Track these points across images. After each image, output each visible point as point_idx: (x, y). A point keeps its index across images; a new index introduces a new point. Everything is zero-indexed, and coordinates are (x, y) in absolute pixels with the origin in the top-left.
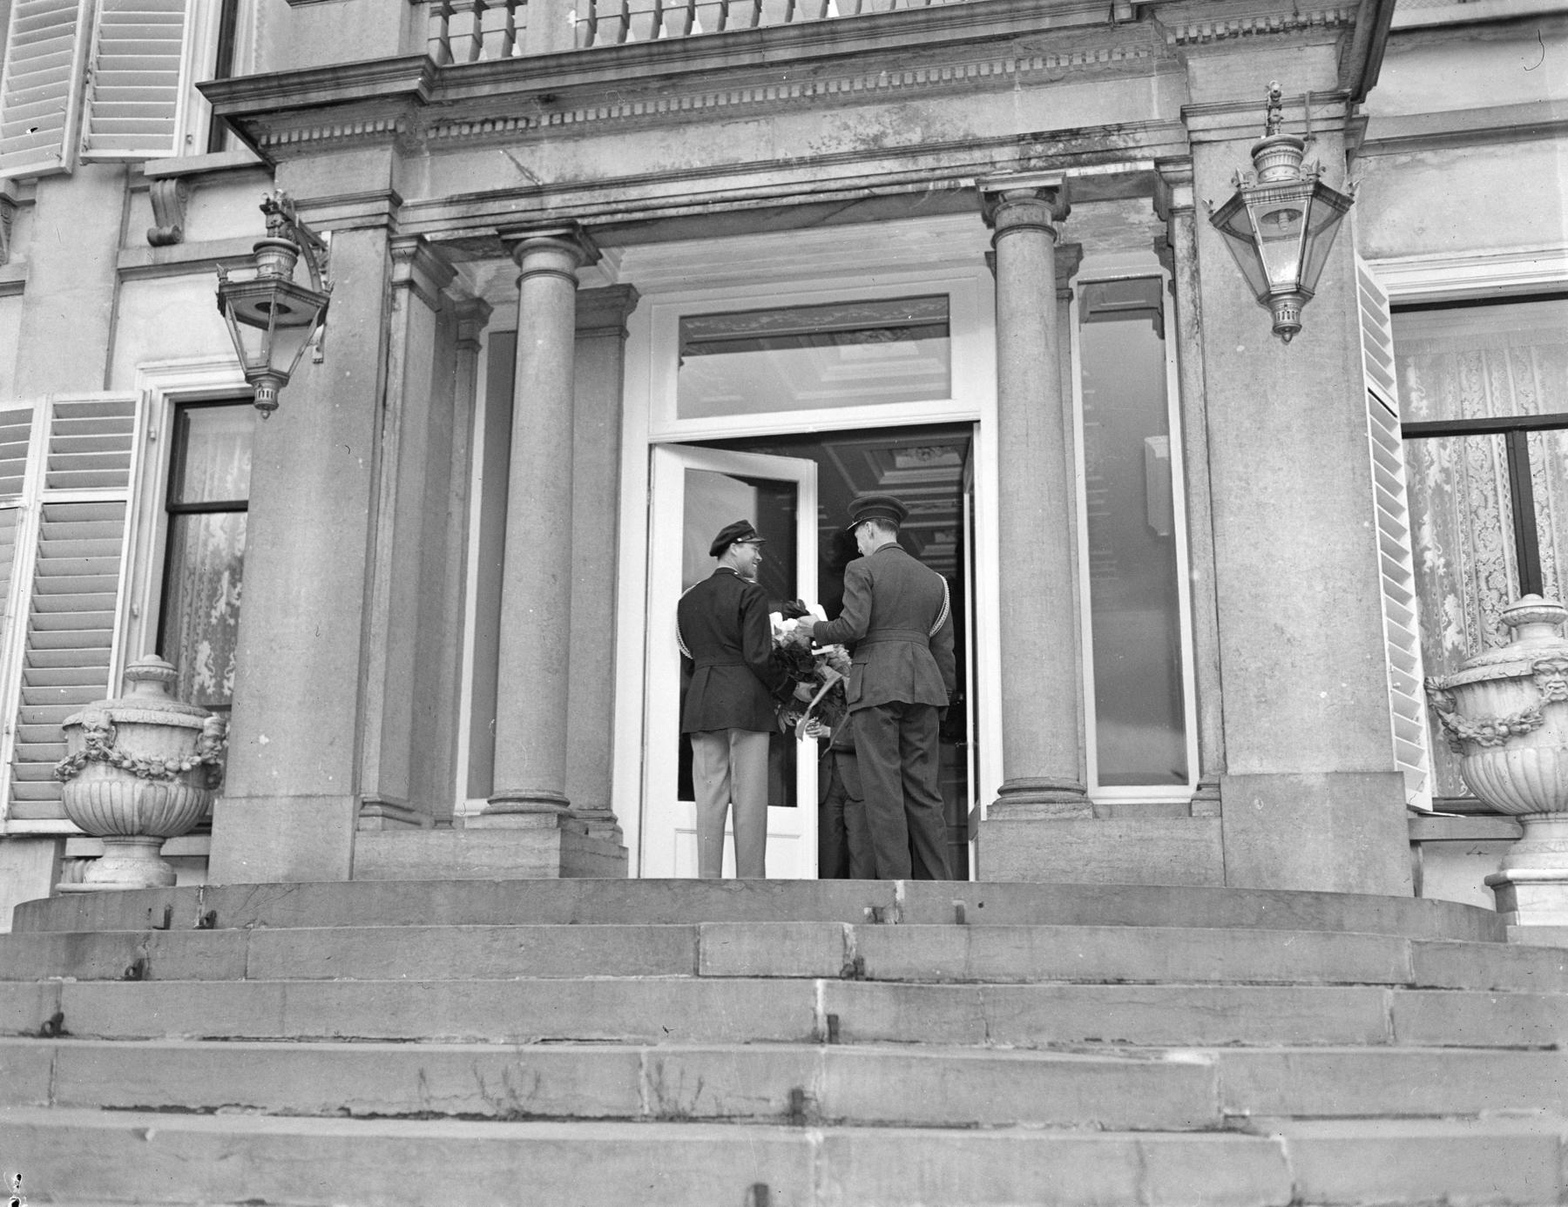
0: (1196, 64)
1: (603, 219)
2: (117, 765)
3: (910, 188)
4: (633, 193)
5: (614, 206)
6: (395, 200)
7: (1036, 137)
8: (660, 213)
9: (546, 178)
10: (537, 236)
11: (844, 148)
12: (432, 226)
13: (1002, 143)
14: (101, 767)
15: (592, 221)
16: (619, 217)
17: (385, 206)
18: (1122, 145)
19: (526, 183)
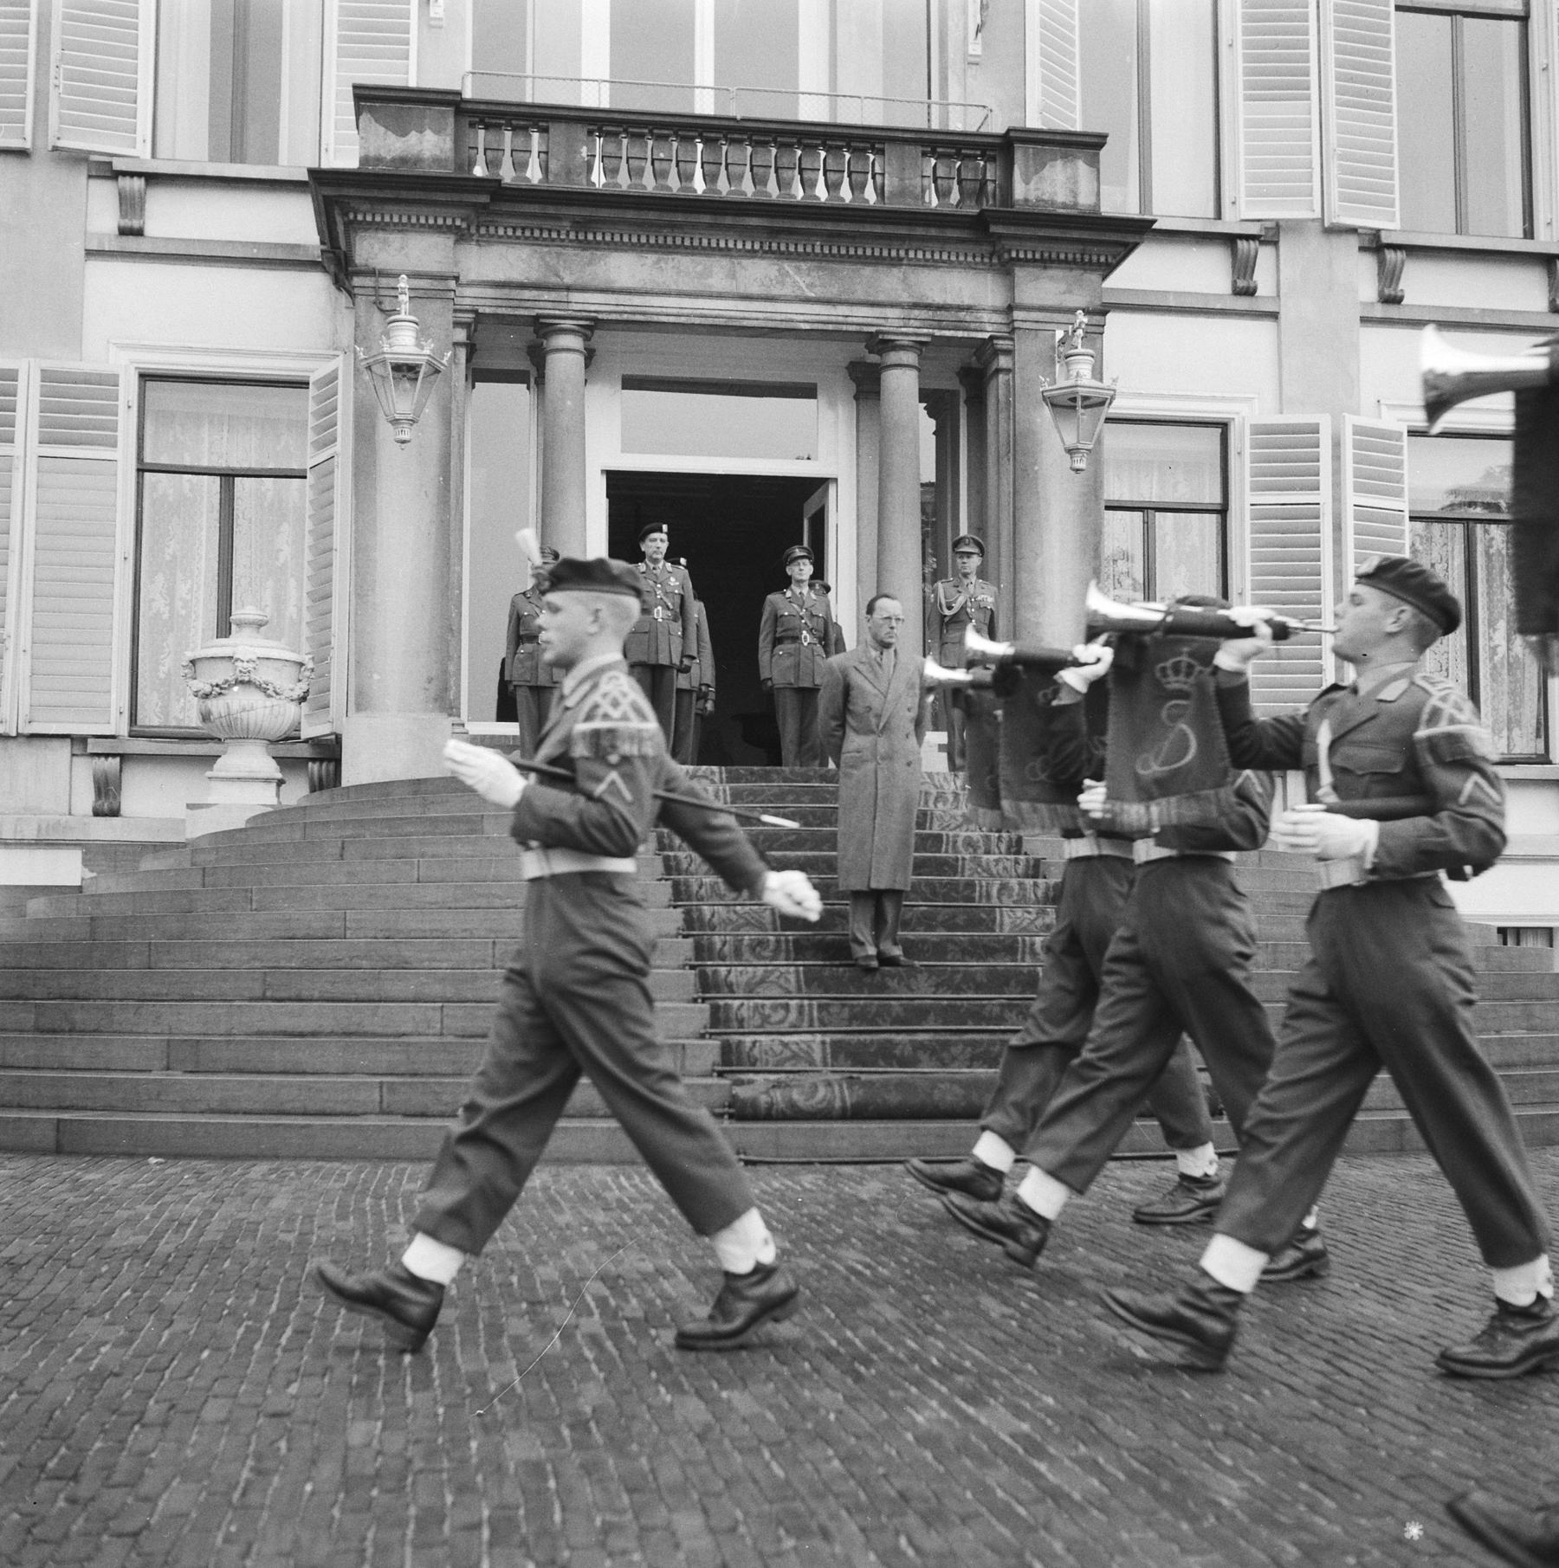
0: (1020, 273)
1: (614, 317)
3: (830, 327)
4: (637, 300)
5: (621, 308)
6: (457, 278)
7: (915, 306)
8: (655, 318)
9: (568, 279)
10: (568, 324)
11: (787, 291)
12: (483, 302)
13: (892, 305)
15: (605, 316)
16: (625, 317)
17: (452, 284)
18: (968, 318)
19: (553, 280)
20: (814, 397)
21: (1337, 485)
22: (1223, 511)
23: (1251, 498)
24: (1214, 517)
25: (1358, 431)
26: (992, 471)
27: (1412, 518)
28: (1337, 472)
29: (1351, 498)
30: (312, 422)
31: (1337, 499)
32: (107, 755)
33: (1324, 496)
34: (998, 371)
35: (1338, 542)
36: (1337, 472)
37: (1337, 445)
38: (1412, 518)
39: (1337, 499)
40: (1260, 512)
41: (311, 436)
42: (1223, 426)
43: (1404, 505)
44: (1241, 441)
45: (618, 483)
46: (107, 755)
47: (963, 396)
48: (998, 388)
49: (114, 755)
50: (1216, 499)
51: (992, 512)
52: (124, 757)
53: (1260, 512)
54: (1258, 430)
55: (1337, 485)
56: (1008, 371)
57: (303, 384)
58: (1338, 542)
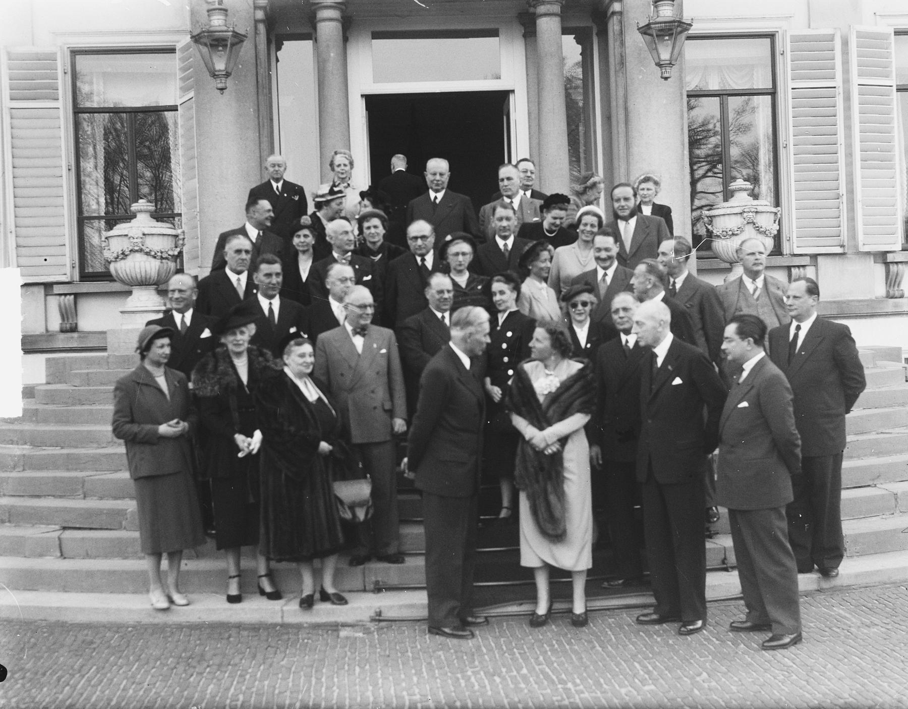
2: (148, 254)
20: (497, 35)
21: (846, 71)
22: (773, 93)
24: (770, 97)
25: (860, 35)
26: (612, 79)
27: (898, 90)
28: (846, 63)
29: (856, 80)
30: (179, 75)
31: (846, 81)
32: (65, 295)
33: (838, 82)
34: (614, 13)
35: (848, 109)
36: (846, 63)
37: (845, 43)
38: (898, 90)
39: (846, 81)
41: (179, 84)
42: (771, 36)
43: (894, 82)
44: (784, 44)
45: (373, 102)
46: (65, 295)
47: (595, 32)
48: (613, 26)
49: (70, 294)
51: (613, 104)
52: (76, 295)
54: (796, 39)
55: (846, 71)
56: (621, 13)
57: (172, 50)
58: (848, 109)
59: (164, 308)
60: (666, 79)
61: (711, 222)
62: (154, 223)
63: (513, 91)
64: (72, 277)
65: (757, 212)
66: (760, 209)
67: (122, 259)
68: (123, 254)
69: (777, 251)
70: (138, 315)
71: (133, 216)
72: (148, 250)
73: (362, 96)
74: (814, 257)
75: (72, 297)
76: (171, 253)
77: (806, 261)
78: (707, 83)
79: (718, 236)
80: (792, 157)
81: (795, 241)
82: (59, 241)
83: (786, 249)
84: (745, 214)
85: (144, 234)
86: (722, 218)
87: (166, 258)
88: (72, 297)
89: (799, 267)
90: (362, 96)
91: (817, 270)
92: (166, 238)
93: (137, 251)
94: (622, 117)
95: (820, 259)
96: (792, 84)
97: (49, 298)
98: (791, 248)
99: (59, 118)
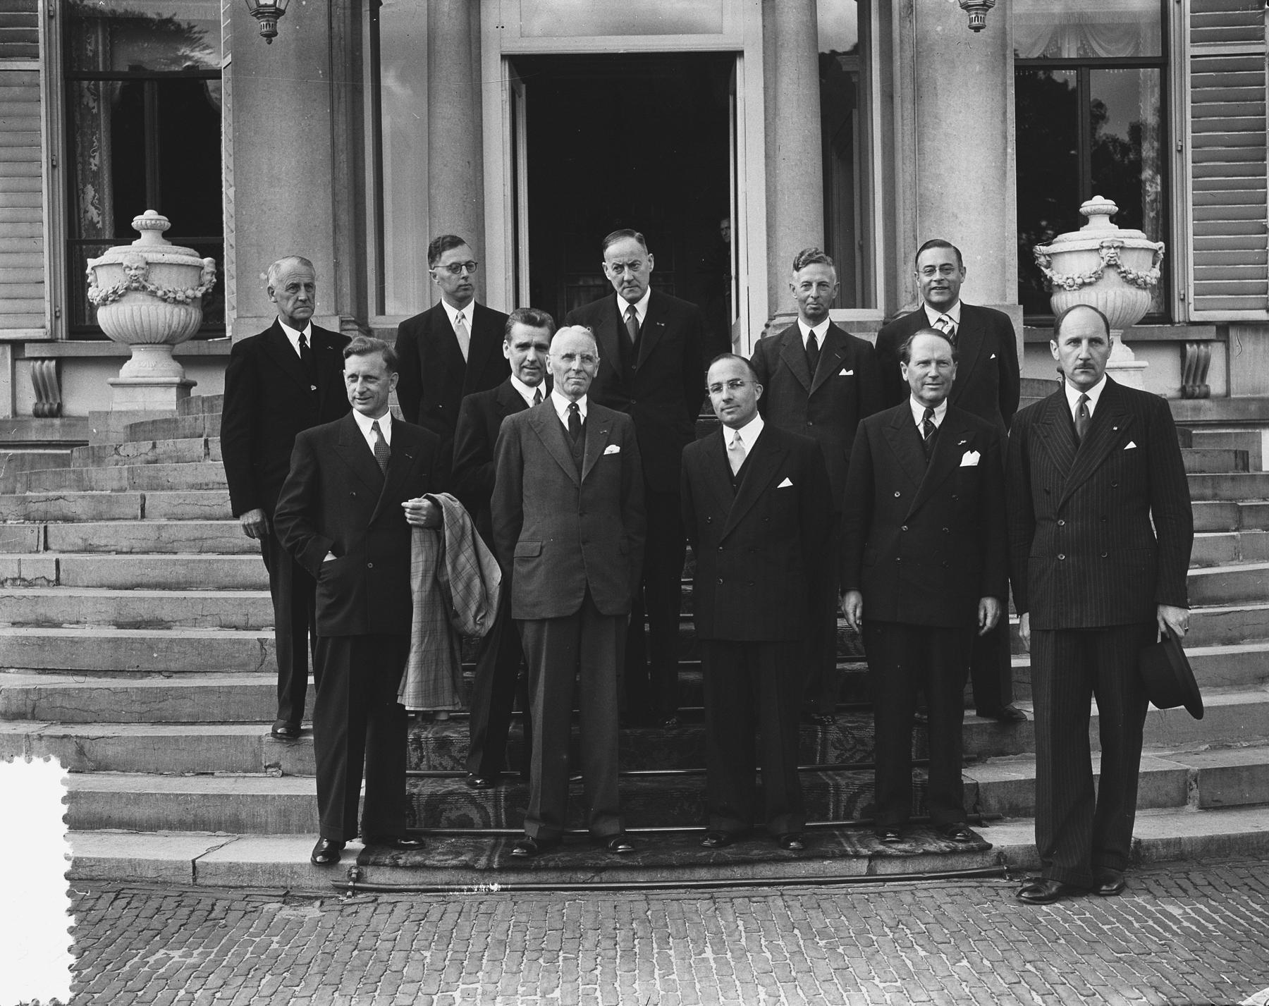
2: (153, 294)
14: (140, 296)
23: (1191, 50)
32: (43, 359)
40: (1199, 65)
46: (43, 359)
49: (50, 359)
50: (1158, 53)
52: (61, 362)
53: (1199, 65)
59: (177, 380)
60: (977, 29)
61: (1049, 266)
62: (169, 247)
63: (741, 53)
64: (54, 330)
65: (1122, 248)
66: (1128, 243)
67: (113, 301)
68: (115, 292)
69: (1163, 314)
70: (138, 390)
71: (138, 236)
72: (152, 288)
73: (504, 57)
74: (1224, 328)
75: (53, 363)
76: (190, 293)
77: (1211, 333)
78: (1060, 49)
79: (1060, 287)
80: (1190, 165)
81: (1191, 300)
82: (33, 275)
83: (1178, 315)
84: (1104, 251)
85: (147, 263)
86: (1067, 256)
87: (182, 302)
88: (53, 363)
89: (1198, 342)
90: (504, 57)
91: (1228, 349)
92: (184, 270)
93: (136, 289)
94: (909, 92)
95: (1233, 334)
96: (1191, 50)
97: (19, 364)
98: (1186, 311)
99: (38, 85)
